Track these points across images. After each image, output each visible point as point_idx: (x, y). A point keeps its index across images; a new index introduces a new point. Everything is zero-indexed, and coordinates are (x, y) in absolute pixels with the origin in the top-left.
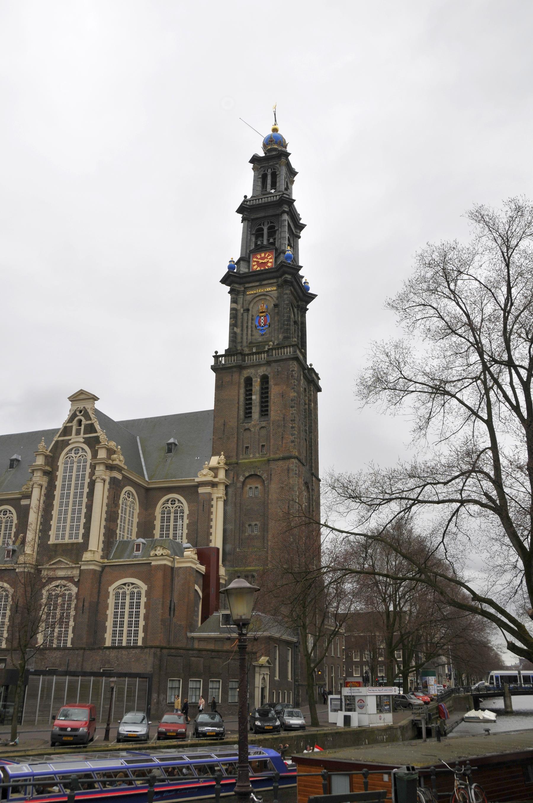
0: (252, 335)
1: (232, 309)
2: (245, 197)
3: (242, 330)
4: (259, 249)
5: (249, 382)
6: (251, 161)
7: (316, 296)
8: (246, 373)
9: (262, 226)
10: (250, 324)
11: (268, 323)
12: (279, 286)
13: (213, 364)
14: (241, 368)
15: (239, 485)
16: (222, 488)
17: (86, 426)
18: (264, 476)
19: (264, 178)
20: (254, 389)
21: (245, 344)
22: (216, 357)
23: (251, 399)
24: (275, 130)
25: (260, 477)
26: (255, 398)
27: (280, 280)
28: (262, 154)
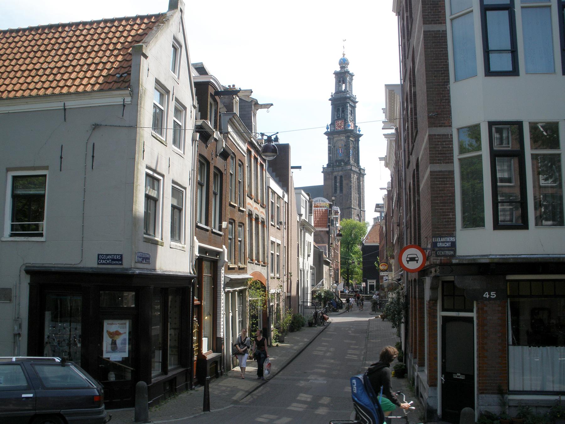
0: (337, 157)
1: (329, 147)
2: (332, 93)
3: (333, 155)
4: (339, 119)
5: (335, 177)
6: (334, 74)
7: (363, 135)
12: (345, 137)
13: (322, 171)
19: (340, 82)
20: (337, 181)
21: (334, 161)
22: (323, 168)
24: (344, 55)
28: (338, 69)
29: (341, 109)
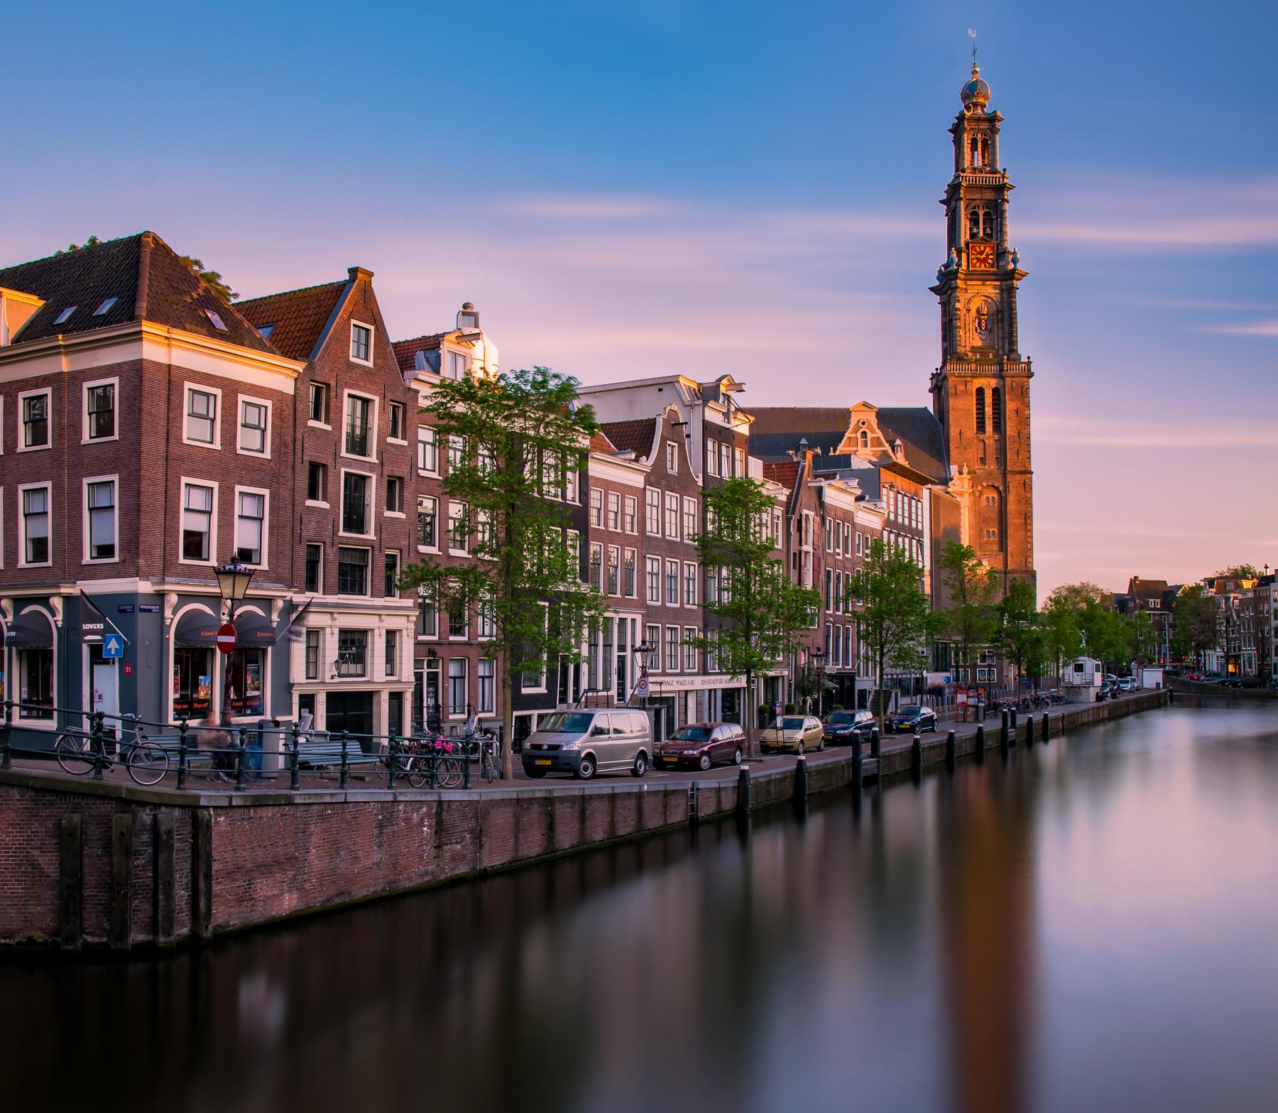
5: (980, 391)
8: (978, 383)
9: (977, 210)
10: (971, 326)
11: (989, 327)
12: (1002, 290)
14: (974, 377)
15: (977, 494)
16: (966, 496)
17: (872, 439)
18: (1001, 489)
21: (968, 348)
23: (983, 409)
25: (997, 488)
26: (988, 410)
27: (1004, 283)
29: (981, 213)
